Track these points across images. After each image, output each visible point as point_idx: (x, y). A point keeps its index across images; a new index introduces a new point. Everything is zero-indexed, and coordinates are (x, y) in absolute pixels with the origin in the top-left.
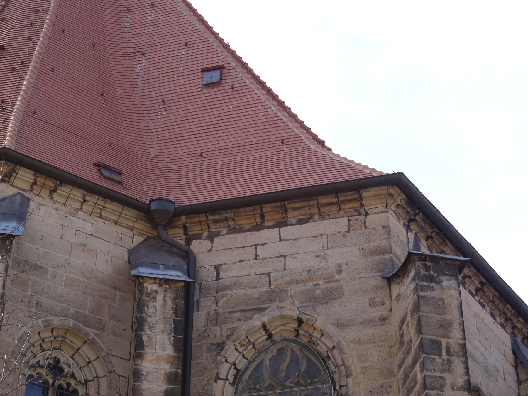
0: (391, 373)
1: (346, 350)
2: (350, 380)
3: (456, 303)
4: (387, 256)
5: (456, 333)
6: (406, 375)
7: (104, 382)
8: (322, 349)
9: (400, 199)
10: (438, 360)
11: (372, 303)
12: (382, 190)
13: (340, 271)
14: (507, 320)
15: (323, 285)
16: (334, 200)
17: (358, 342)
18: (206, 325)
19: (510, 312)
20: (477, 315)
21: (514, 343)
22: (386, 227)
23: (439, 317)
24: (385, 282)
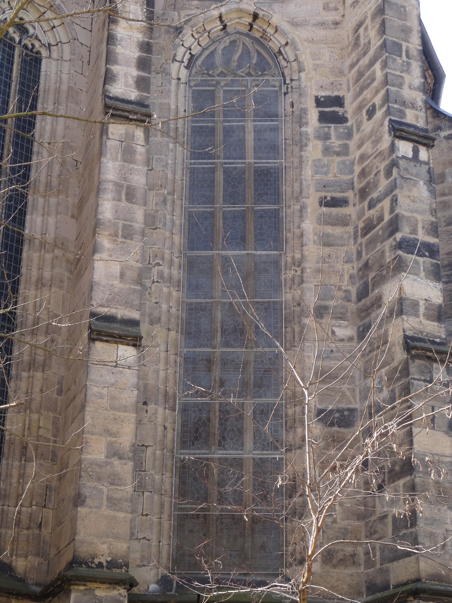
7: (67, 48)
18: (165, 9)
23: (400, 22)
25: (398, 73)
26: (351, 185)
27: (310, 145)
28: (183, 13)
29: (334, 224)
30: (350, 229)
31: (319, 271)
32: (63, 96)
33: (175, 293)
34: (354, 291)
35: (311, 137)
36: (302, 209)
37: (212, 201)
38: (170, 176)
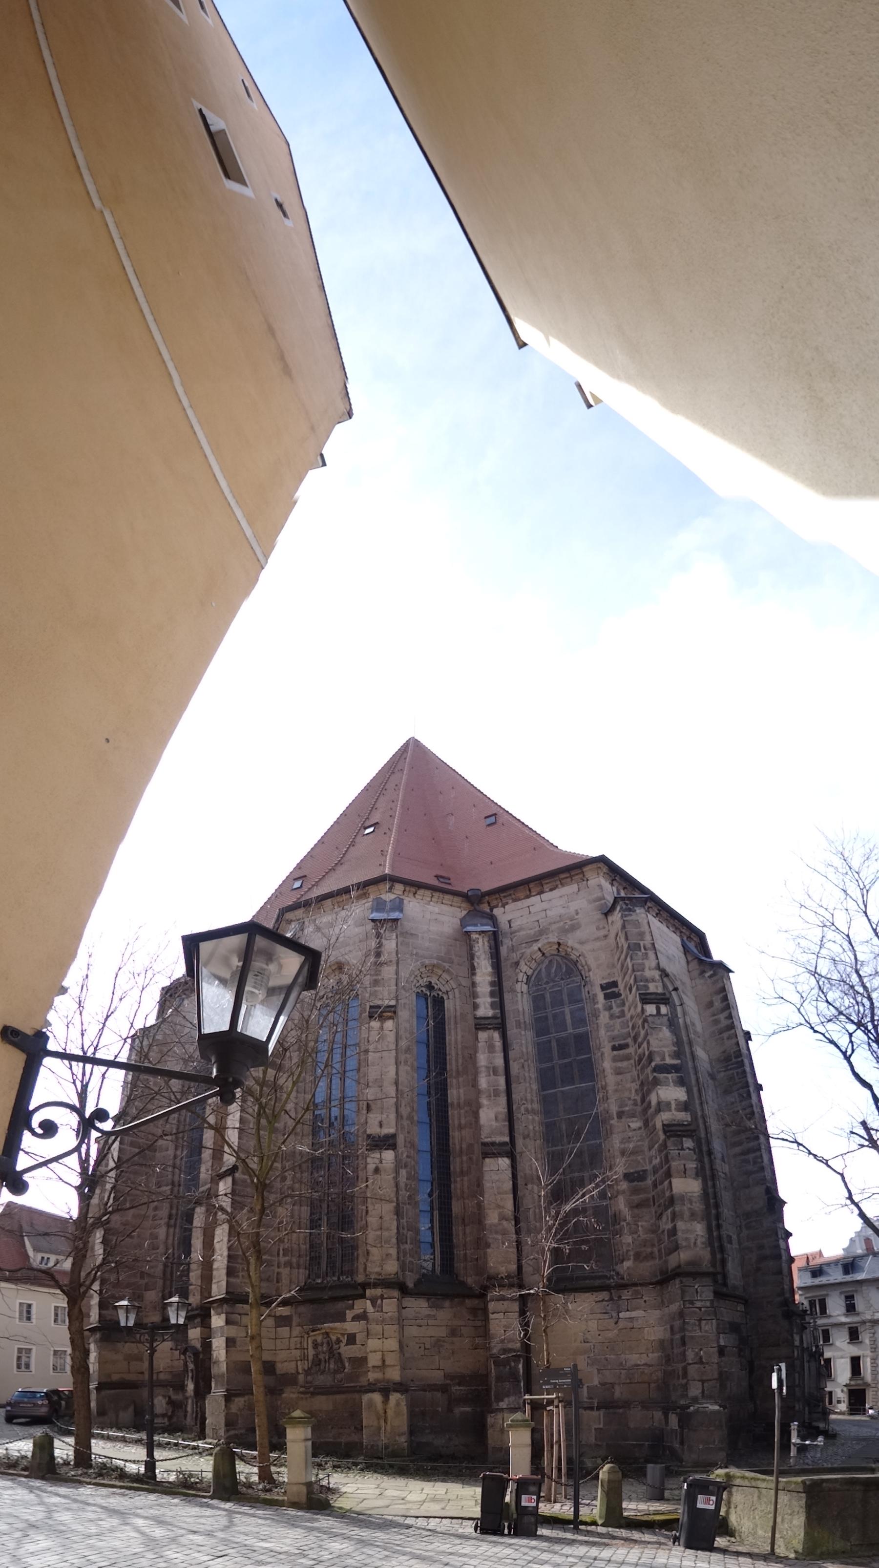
0: (613, 966)
1: (586, 955)
2: (591, 973)
3: (646, 921)
4: (603, 902)
5: (648, 938)
6: (623, 966)
7: (456, 991)
8: (573, 957)
9: (605, 869)
10: (640, 953)
11: (598, 928)
12: (594, 866)
13: (577, 914)
14: (677, 928)
15: (569, 923)
16: (568, 875)
17: (594, 950)
19: (677, 924)
20: (659, 928)
21: (682, 941)
22: (600, 886)
23: (637, 930)
24: (603, 916)
25: (640, 961)
26: (629, 1035)
27: (602, 1016)
28: (518, 953)
29: (621, 1061)
30: (632, 1061)
31: (616, 1091)
32: (458, 1018)
33: (537, 1118)
34: (638, 1098)
35: (601, 1010)
36: (602, 1054)
37: (551, 1059)
38: (524, 1050)
